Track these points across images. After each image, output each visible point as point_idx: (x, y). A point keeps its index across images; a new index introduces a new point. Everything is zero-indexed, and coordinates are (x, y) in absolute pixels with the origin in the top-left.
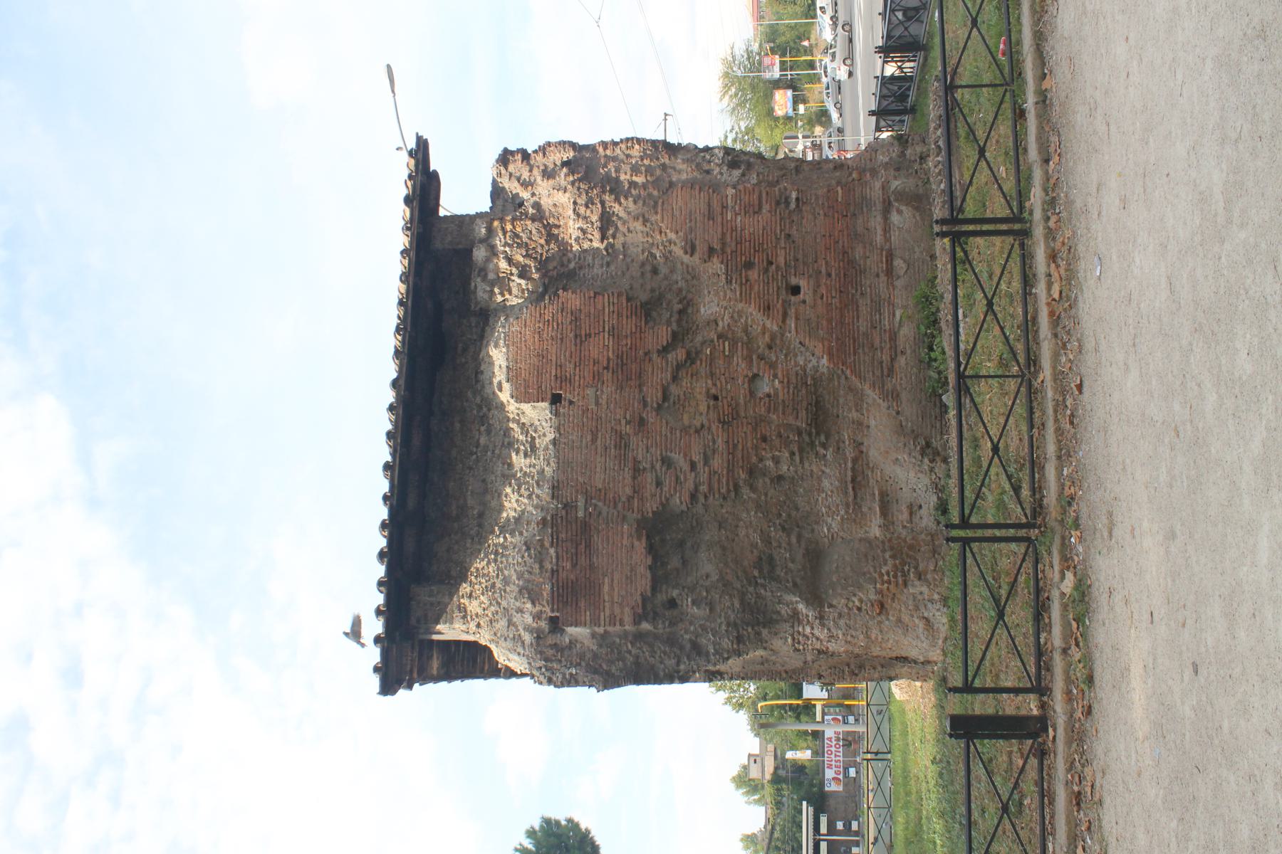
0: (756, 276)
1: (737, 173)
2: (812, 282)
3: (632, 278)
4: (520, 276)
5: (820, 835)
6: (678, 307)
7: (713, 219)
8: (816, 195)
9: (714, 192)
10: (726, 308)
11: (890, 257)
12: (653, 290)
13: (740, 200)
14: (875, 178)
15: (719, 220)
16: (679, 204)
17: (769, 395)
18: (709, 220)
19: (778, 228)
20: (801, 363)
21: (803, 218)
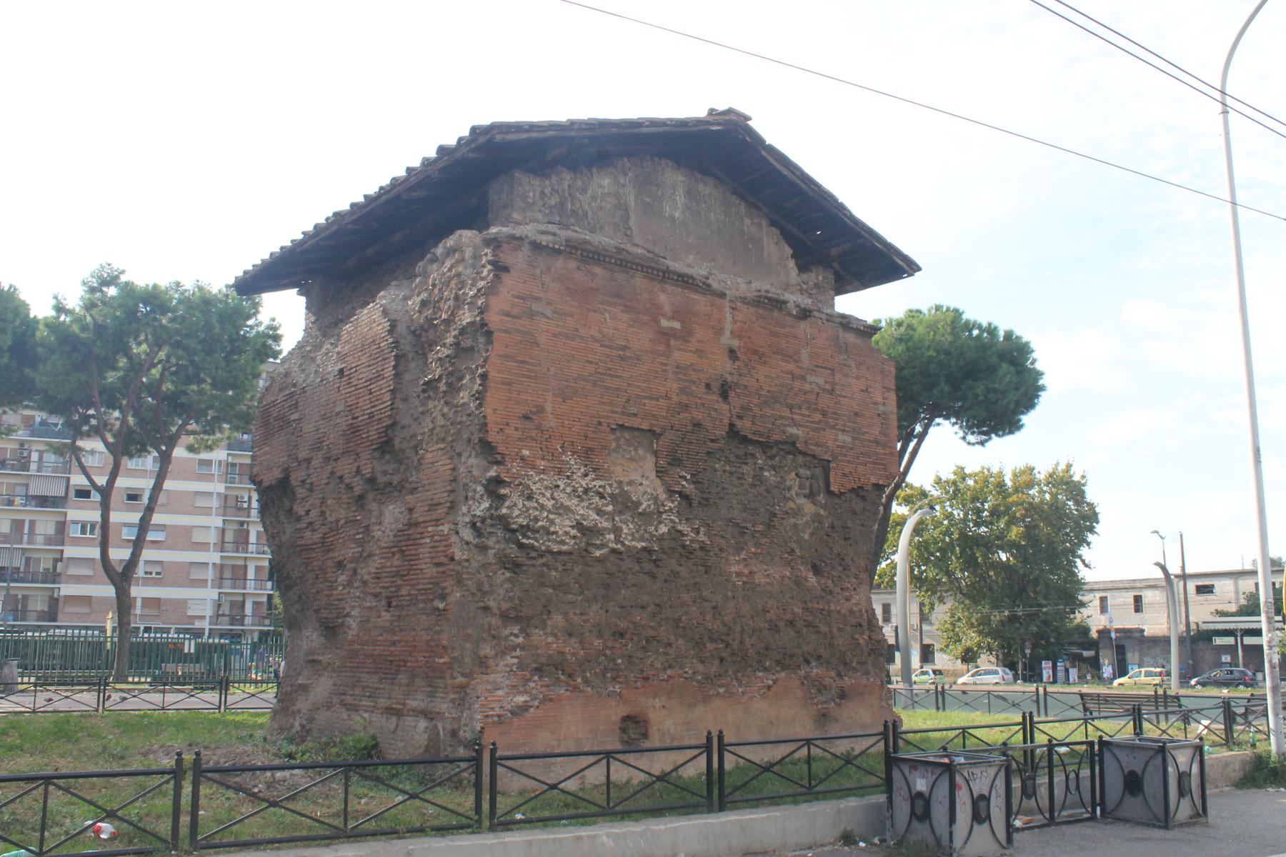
0: (396, 563)
1: (467, 534)
2: (387, 624)
3: (410, 426)
4: (424, 304)
5: (1242, 636)
6: (395, 479)
7: (429, 510)
8: (442, 631)
9: (449, 508)
10: (384, 532)
11: (398, 713)
12: (403, 451)
13: (440, 541)
14: (451, 705)
15: (428, 518)
16: (441, 469)
17: (336, 581)
18: (430, 505)
19: (420, 587)
20: (353, 613)
21: (428, 615)
